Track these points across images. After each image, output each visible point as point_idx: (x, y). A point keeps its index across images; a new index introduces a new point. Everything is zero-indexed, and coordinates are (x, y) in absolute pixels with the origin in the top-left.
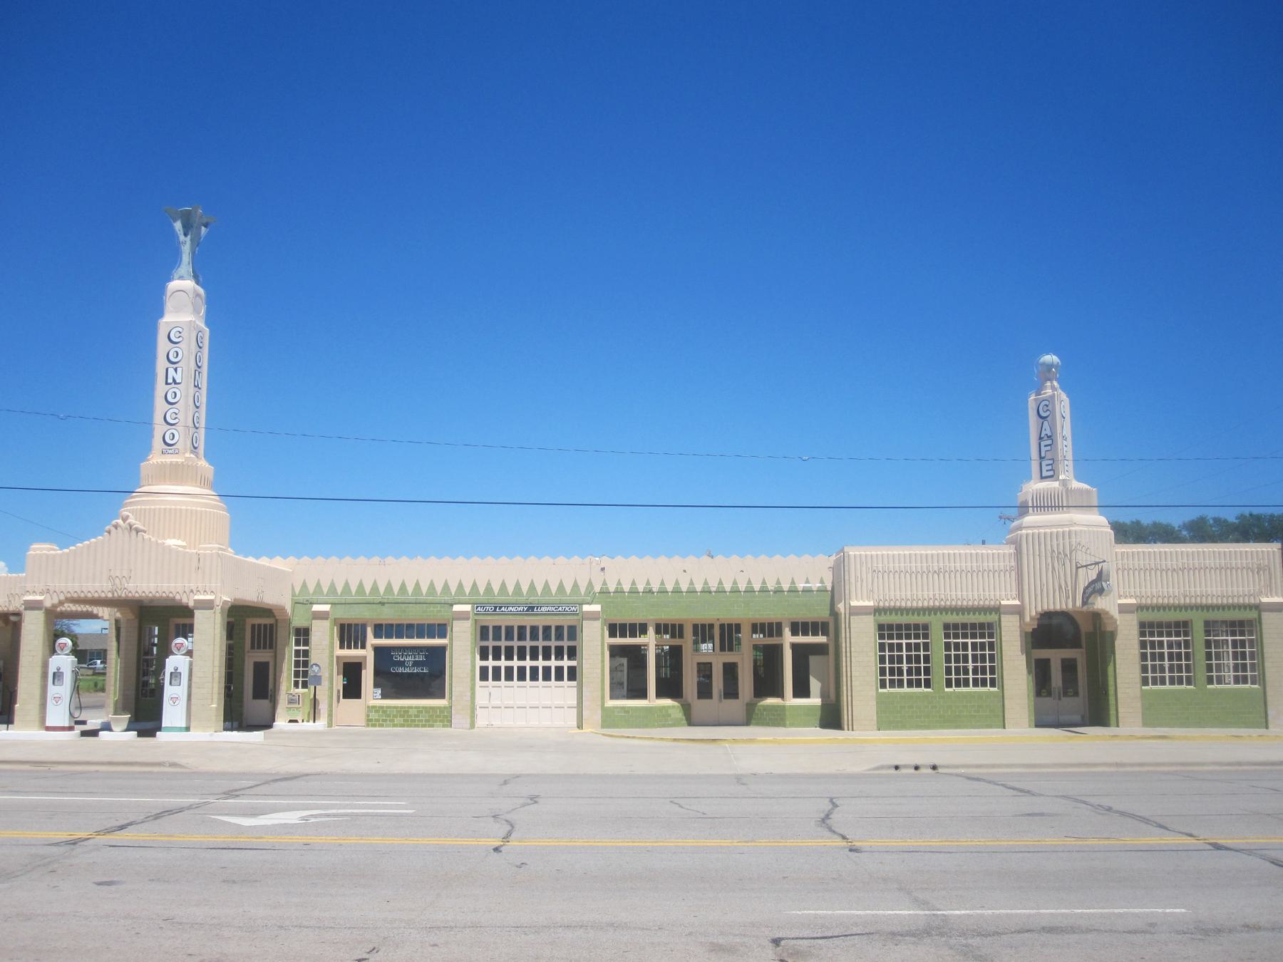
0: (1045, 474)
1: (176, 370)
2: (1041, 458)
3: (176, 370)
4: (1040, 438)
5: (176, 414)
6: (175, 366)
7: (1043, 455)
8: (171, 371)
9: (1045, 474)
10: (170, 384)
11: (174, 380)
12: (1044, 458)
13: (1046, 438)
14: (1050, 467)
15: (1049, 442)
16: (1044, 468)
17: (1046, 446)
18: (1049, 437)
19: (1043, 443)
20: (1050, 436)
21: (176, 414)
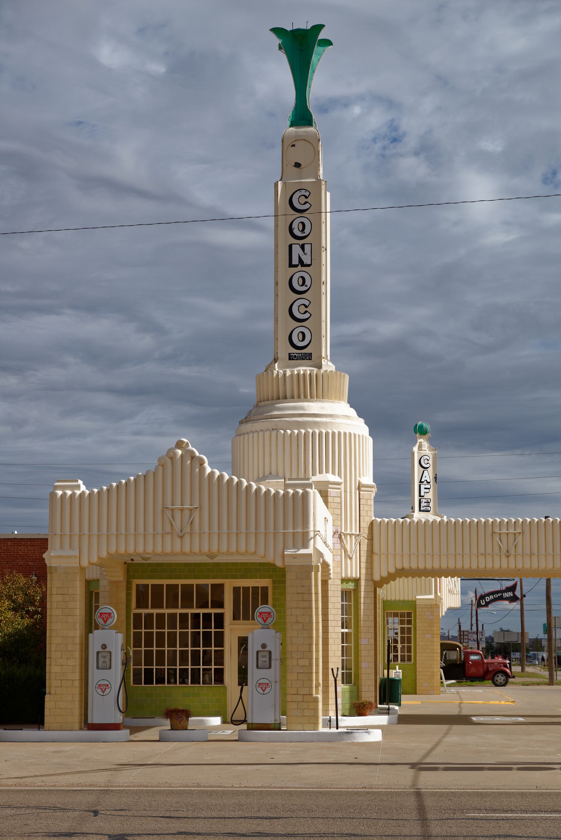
0: (422, 509)
1: (302, 247)
2: (420, 496)
3: (302, 247)
4: (421, 482)
5: (306, 307)
6: (301, 242)
7: (422, 494)
8: (296, 250)
9: (422, 509)
10: (296, 266)
11: (301, 261)
12: (423, 496)
13: (425, 483)
14: (426, 504)
15: (428, 486)
16: (423, 504)
17: (425, 488)
18: (428, 483)
19: (423, 487)
20: (429, 483)
21: (306, 307)
